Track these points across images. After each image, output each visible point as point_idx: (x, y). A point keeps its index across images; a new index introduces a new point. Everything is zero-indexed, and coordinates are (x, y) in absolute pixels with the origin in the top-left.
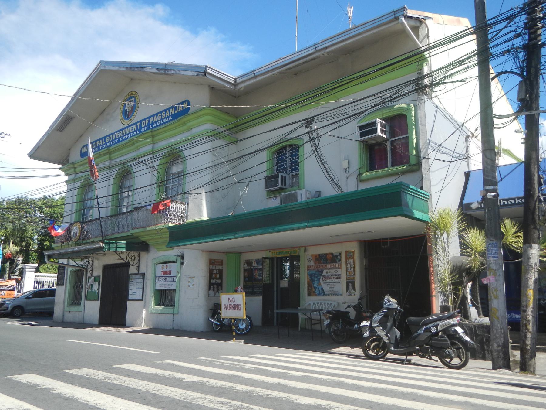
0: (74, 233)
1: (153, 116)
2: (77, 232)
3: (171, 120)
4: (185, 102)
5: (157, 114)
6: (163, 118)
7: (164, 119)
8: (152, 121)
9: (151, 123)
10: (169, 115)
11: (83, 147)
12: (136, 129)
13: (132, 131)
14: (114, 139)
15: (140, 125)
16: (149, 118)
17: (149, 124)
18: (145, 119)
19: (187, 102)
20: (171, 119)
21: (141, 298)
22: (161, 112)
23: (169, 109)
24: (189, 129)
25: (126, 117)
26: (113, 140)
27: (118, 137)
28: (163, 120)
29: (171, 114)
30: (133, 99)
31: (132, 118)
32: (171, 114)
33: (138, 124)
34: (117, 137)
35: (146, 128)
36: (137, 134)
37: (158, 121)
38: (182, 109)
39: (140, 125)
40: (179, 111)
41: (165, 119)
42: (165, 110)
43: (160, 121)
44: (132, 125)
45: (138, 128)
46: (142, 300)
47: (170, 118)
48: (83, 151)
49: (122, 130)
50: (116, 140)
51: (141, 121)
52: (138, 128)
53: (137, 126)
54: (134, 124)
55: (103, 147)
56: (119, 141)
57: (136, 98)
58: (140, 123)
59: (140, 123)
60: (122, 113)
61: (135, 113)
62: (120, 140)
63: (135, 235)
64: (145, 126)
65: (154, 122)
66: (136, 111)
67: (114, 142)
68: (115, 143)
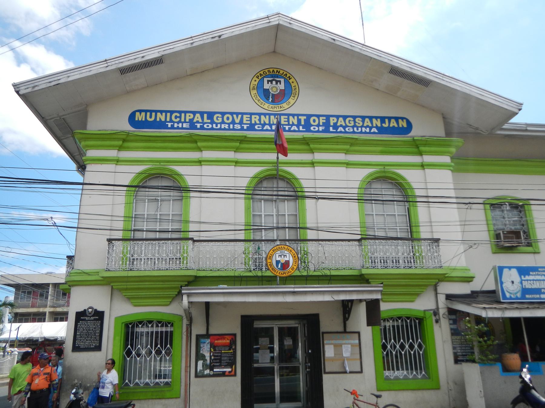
0: (278, 262)
1: (338, 117)
2: (287, 262)
3: (374, 133)
4: (402, 119)
5: (345, 117)
6: (357, 124)
7: (362, 127)
8: (335, 124)
9: (332, 124)
10: (370, 125)
11: (140, 111)
12: (296, 123)
13: (287, 123)
14: (237, 121)
15: (305, 120)
16: (328, 117)
17: (327, 124)
18: (318, 116)
19: (405, 120)
20: (376, 131)
21: (359, 370)
22: (354, 117)
23: (371, 118)
24: (421, 154)
25: (268, 100)
26: (233, 122)
27: (249, 122)
28: (360, 129)
29: (374, 125)
30: (282, 80)
31: (285, 105)
32: (374, 125)
33: (303, 118)
34: (245, 122)
35: (321, 129)
36: (299, 131)
37: (347, 126)
38: (396, 126)
39: (307, 121)
40: (391, 125)
41: (364, 129)
42: (363, 118)
43: (353, 127)
44: (289, 115)
45: (303, 123)
46: (361, 372)
47: (374, 130)
48: (140, 117)
49: (260, 115)
50: (245, 127)
51: (309, 116)
52: (303, 123)
53: (299, 121)
54: (293, 115)
55: (205, 126)
56: (251, 127)
57: (291, 81)
58: (305, 117)
59: (305, 117)
60: (255, 91)
61: (291, 101)
62: (256, 127)
63: (366, 276)
64: (318, 125)
65: (339, 124)
66: (292, 97)
67: (238, 127)
68: (242, 129)
